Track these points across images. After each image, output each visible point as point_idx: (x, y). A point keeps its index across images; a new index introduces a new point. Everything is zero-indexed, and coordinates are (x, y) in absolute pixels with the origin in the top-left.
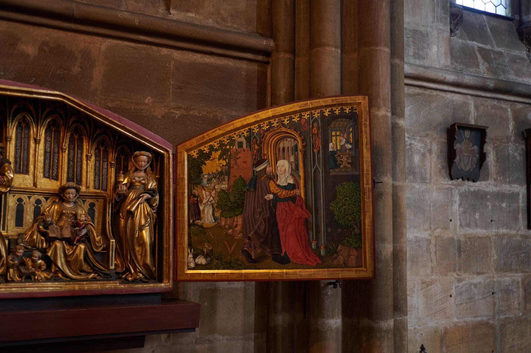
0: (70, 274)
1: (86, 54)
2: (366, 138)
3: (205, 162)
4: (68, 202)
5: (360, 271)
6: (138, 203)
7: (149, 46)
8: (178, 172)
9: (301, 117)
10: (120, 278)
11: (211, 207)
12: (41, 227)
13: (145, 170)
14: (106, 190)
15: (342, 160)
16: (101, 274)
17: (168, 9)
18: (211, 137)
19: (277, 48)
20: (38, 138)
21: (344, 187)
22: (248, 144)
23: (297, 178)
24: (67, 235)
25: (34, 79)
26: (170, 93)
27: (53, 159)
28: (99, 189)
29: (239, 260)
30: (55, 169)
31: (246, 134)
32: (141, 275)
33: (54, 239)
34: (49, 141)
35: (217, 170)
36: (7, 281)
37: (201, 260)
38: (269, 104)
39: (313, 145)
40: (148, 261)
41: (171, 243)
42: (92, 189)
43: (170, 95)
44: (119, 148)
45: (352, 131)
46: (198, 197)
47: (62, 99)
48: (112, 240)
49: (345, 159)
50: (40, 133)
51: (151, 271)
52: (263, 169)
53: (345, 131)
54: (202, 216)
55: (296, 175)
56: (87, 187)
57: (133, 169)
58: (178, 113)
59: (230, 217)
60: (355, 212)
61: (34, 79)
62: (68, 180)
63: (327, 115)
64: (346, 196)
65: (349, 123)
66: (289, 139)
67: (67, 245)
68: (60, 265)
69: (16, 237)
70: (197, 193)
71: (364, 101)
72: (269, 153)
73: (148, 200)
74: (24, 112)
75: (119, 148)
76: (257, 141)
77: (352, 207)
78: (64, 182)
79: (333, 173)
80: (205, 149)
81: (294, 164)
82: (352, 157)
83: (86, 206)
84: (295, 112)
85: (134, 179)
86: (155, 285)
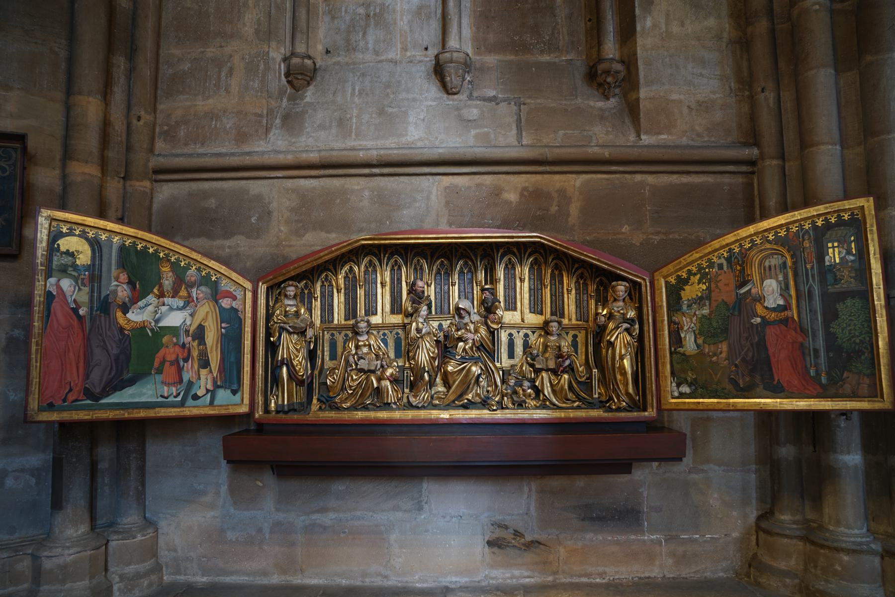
0: (556, 402)
1: (562, 192)
2: (874, 246)
3: (684, 287)
4: (552, 335)
5: (875, 401)
6: (617, 333)
7: (622, 175)
8: (656, 300)
9: (788, 230)
10: (604, 406)
11: (693, 334)
12: (529, 359)
13: (624, 300)
14: (587, 321)
15: (843, 274)
16: (586, 403)
17: (639, 136)
18: (688, 261)
19: (762, 156)
20: (523, 277)
21: (847, 306)
22: (729, 266)
23: (788, 298)
25: (518, 222)
27: (537, 295)
28: (581, 321)
29: (725, 389)
31: (726, 255)
32: (624, 403)
33: (540, 370)
35: (697, 295)
36: (503, 408)
37: (685, 389)
38: (758, 217)
39: (805, 260)
40: (631, 390)
41: (653, 372)
42: (574, 322)
44: (598, 279)
45: (854, 240)
46: (678, 324)
47: (539, 240)
48: (594, 370)
49: (847, 273)
51: (634, 399)
52: (747, 291)
53: (845, 241)
54: (683, 343)
55: (786, 295)
56: (570, 320)
57: (612, 299)
58: (657, 238)
59: (714, 344)
60: (863, 333)
61: (518, 222)
62: (552, 314)
63: (820, 225)
64: (850, 316)
65: (850, 232)
66: (775, 256)
68: (546, 393)
69: (509, 369)
70: (677, 320)
71: (868, 204)
72: (754, 273)
73: (627, 330)
75: (598, 279)
76: (739, 261)
77: (859, 328)
78: (548, 315)
79: (831, 289)
80: (683, 274)
81: (783, 282)
82: (855, 270)
83: (570, 338)
84: (781, 226)
85: (613, 309)
86: (639, 413)
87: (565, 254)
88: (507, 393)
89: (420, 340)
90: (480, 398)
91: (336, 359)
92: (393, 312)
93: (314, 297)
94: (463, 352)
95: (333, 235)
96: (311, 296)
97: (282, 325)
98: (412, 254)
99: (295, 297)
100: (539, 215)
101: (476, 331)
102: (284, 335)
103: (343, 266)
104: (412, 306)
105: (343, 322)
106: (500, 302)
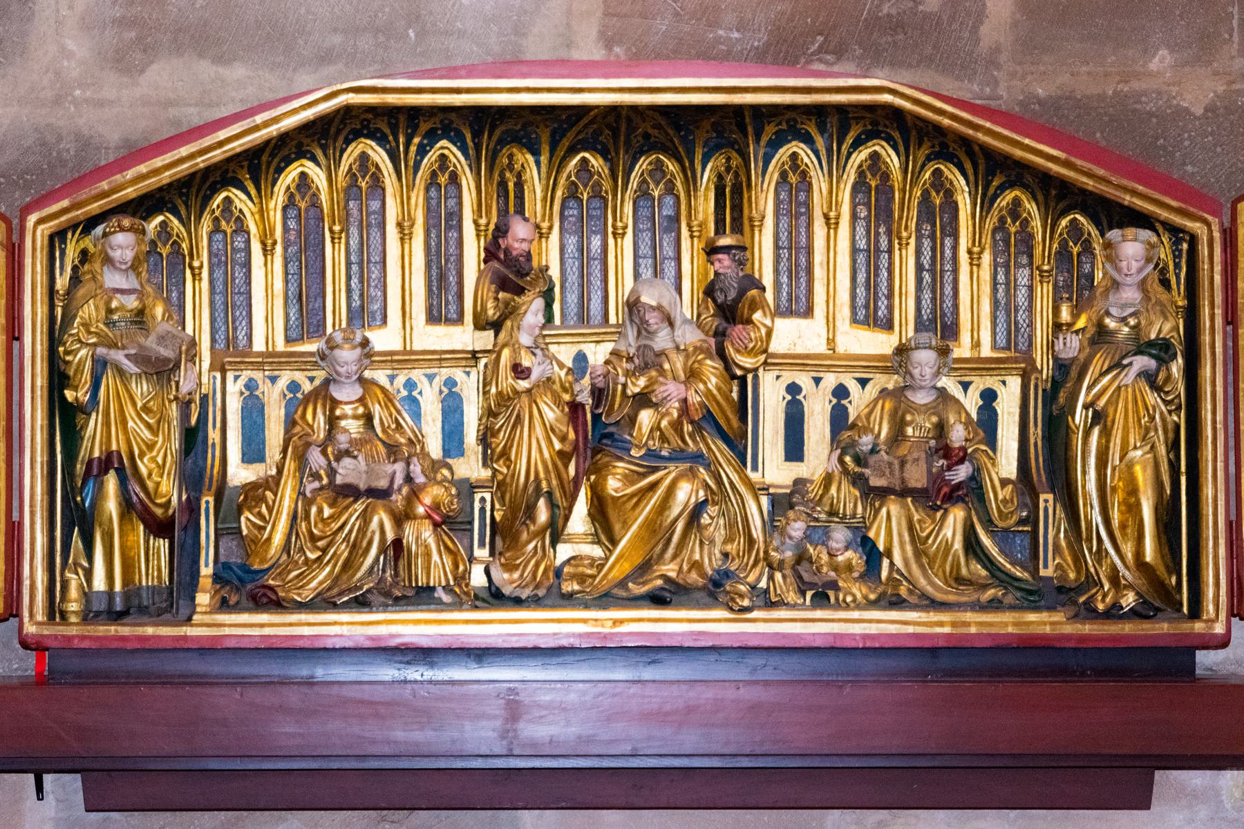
24: (917, 480)
25: (820, 39)
26: (1233, 30)
28: (1009, 349)
30: (883, 298)
34: (864, 219)
36: (771, 605)
40: (1149, 554)
43: (1231, 36)
44: (1064, 222)
48: (1042, 497)
50: (837, 196)
61: (820, 39)
62: (920, 326)
67: (920, 510)
74: (794, 143)
85: (1108, 313)
87: (966, 142)
88: (782, 562)
89: (525, 399)
90: (702, 574)
91: (261, 459)
92: (434, 317)
93: (192, 268)
94: (651, 436)
95: (238, 71)
96: (179, 262)
97: (101, 351)
98: (495, 138)
99: (134, 267)
100: (889, 15)
101: (693, 375)
102: (109, 381)
103: (280, 171)
104: (496, 299)
105: (281, 346)
106: (764, 289)
